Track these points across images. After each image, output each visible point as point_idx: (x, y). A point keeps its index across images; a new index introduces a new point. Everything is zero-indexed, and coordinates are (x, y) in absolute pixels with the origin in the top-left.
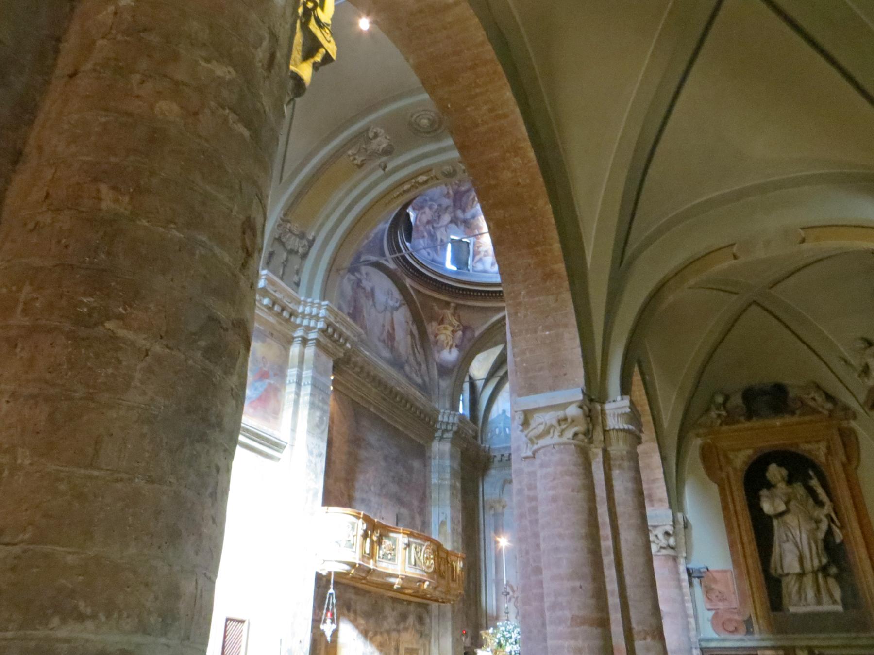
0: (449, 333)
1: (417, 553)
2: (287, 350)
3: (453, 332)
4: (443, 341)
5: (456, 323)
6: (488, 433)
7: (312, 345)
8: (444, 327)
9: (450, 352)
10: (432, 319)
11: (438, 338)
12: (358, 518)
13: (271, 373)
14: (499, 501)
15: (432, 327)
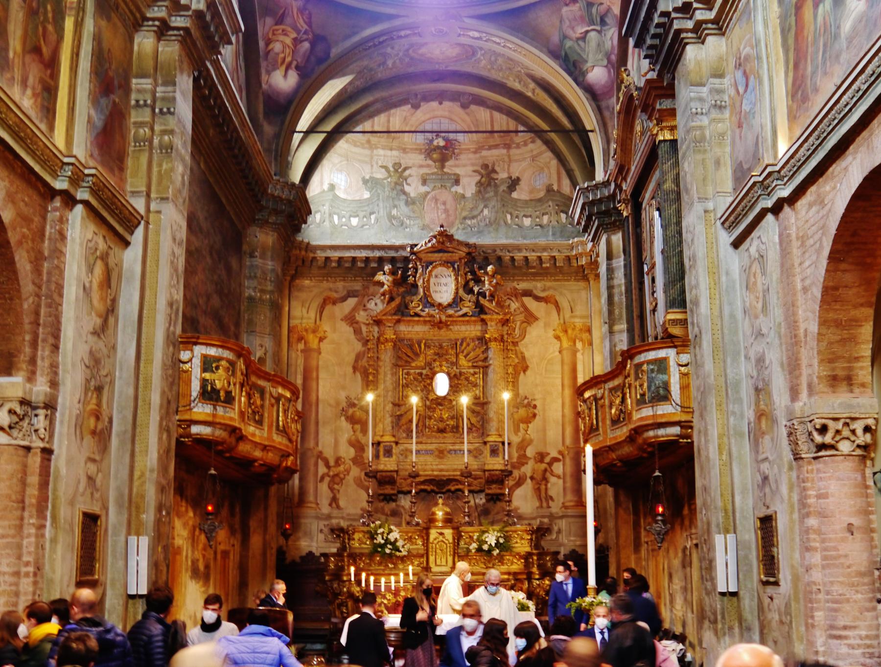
0: (288, 41)
1: (285, 411)
2: (131, 40)
3: (296, 42)
4: (278, 54)
5: (302, 25)
7: (174, 38)
8: (283, 31)
9: (285, 76)
10: (268, 11)
11: (271, 47)
12: (239, 355)
13: (116, 83)
14: (314, 331)
15: (264, 26)
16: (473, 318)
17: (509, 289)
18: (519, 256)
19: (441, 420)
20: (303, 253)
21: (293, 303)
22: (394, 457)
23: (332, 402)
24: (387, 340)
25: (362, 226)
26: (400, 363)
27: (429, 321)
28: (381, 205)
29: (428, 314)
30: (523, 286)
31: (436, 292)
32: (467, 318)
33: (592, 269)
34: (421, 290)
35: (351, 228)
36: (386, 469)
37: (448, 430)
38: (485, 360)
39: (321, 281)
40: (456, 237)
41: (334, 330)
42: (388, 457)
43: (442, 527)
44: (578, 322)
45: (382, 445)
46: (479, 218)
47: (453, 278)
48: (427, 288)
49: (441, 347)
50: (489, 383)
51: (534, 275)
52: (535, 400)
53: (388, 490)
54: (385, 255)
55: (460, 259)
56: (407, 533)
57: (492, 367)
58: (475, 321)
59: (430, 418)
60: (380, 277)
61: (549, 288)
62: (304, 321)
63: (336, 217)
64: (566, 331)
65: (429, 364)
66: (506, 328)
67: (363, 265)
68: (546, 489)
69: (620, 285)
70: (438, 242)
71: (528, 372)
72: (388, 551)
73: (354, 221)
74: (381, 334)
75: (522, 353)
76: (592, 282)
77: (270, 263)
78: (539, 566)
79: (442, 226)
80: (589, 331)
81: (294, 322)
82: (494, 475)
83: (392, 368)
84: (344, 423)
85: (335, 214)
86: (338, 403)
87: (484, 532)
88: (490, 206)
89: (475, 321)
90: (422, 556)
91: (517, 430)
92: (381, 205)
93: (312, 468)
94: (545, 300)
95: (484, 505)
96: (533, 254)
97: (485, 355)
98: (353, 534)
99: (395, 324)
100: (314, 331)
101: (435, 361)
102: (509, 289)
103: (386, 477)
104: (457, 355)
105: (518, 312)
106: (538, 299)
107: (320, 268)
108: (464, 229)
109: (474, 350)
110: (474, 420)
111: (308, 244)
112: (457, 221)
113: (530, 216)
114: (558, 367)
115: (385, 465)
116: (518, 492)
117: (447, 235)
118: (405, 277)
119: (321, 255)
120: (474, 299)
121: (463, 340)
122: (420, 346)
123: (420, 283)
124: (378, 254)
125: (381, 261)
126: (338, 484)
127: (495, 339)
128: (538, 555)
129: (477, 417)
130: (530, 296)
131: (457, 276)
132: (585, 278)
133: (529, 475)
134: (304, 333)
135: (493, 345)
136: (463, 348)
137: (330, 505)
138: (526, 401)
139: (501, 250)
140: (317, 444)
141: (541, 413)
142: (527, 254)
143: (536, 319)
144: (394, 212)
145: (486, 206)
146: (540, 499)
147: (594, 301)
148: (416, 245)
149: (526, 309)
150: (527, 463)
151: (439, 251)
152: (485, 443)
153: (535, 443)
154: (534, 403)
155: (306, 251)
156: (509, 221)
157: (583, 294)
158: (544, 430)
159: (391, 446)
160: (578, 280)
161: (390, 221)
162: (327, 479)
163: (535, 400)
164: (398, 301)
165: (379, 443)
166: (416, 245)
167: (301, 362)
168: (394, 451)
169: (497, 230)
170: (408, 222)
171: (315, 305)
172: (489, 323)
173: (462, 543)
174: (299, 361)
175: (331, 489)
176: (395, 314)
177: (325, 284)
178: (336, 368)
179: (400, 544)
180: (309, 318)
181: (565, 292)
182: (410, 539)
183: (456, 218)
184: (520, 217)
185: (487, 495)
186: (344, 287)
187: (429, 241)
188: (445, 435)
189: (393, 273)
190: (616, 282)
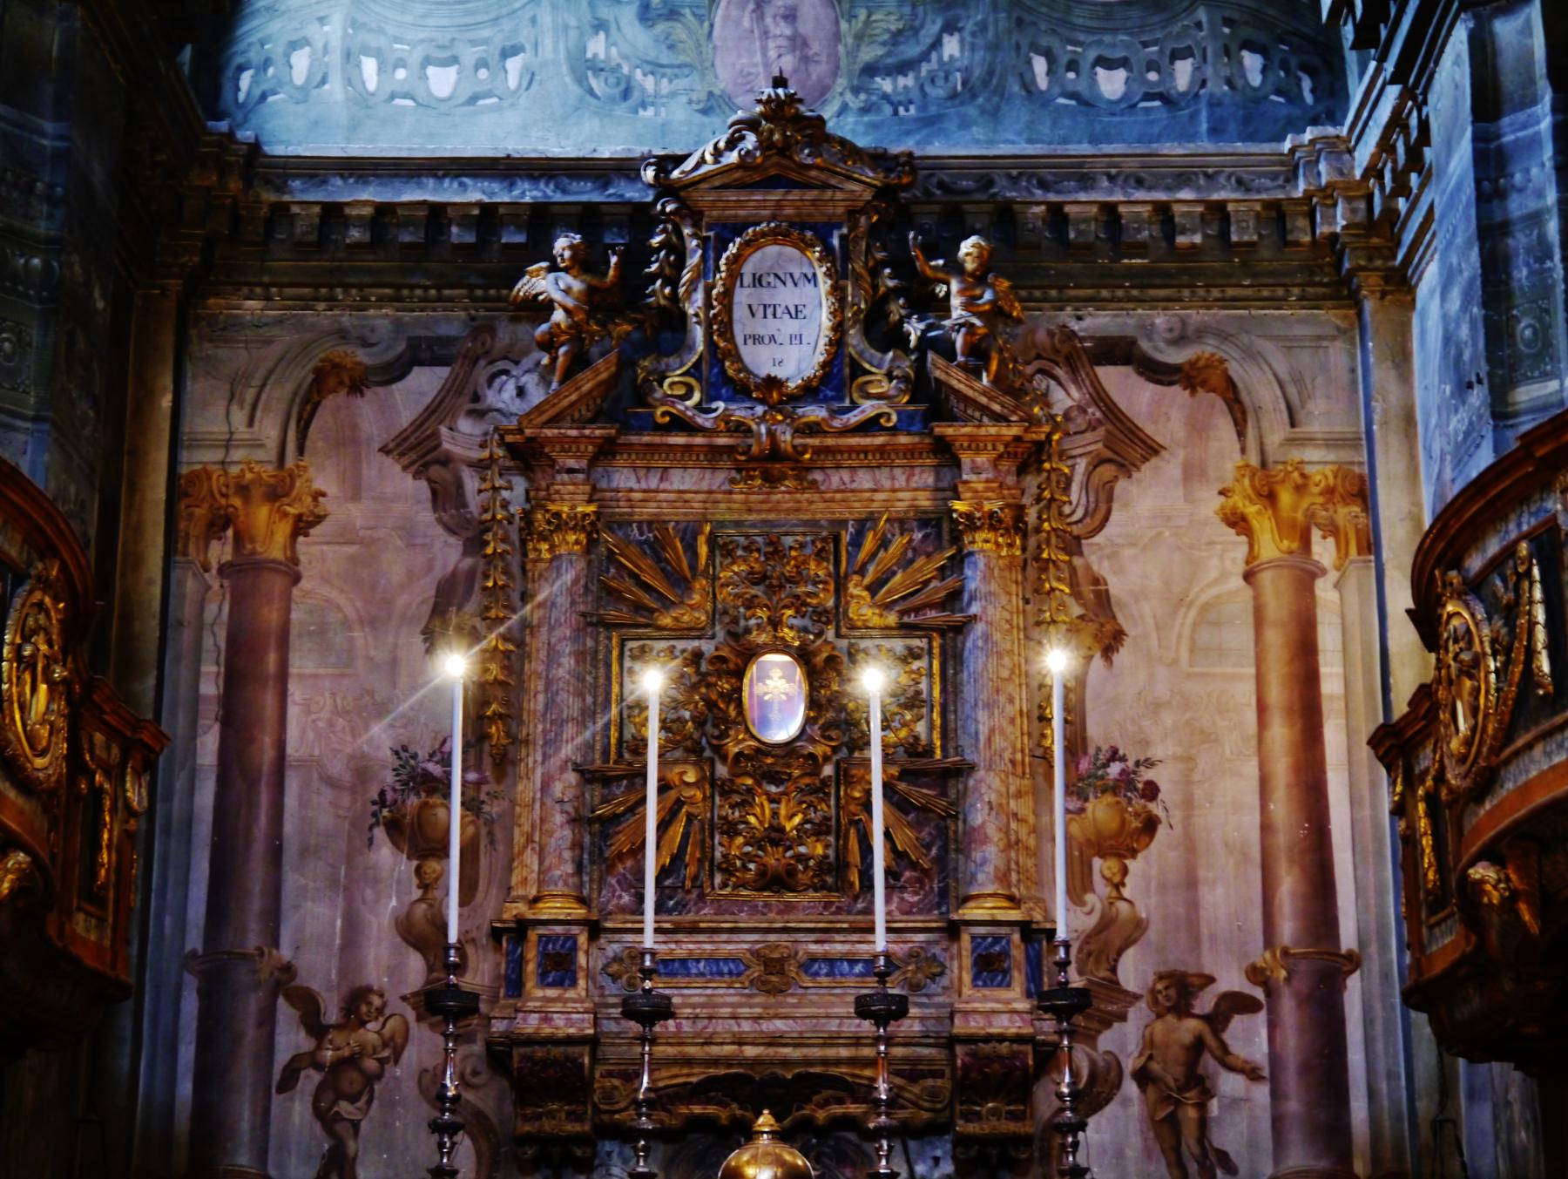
6: (241, 69)
14: (276, 493)
16: (903, 439)
17: (1041, 336)
18: (1082, 202)
19: (775, 836)
20: (235, 184)
21: (196, 387)
22: (582, 983)
23: (338, 767)
24: (559, 524)
25: (473, 99)
26: (612, 613)
27: (730, 450)
28: (546, 19)
29: (725, 418)
30: (1097, 322)
31: (758, 339)
32: (879, 440)
33: (1372, 252)
34: (699, 333)
35: (427, 104)
36: (547, 1030)
37: (803, 878)
38: (954, 597)
39: (307, 303)
40: (832, 126)
41: (355, 491)
42: (555, 984)
44: (1319, 462)
45: (533, 935)
46: (925, 68)
47: (824, 285)
48: (720, 324)
49: (776, 551)
50: (968, 692)
51: (1143, 279)
52: (1150, 763)
53: (559, 1121)
54: (559, 197)
55: (852, 214)
57: (979, 628)
58: (910, 452)
59: (731, 830)
60: (540, 283)
61: (1200, 334)
62: (237, 455)
63: (369, 66)
64: (1270, 498)
66: (1032, 482)
67: (470, 238)
68: (1203, 1123)
69: (1536, 218)
70: (765, 144)
71: (1123, 656)
73: (442, 81)
74: (534, 502)
75: (1096, 581)
76: (1369, 306)
77: (49, 127)
79: (779, 82)
80: (1363, 493)
81: (195, 459)
83: (579, 632)
84: (385, 855)
85: (367, 51)
86: (362, 771)
88: (970, 26)
89: (910, 452)
91: (1079, 885)
92: (546, 19)
94: (1188, 377)
96: (1140, 195)
97: (951, 582)
99: (594, 461)
100: (276, 493)
101: (750, 604)
102: (1041, 336)
103: (548, 1063)
104: (840, 589)
105: (1081, 422)
106: (1156, 372)
107: (302, 249)
108: (865, 110)
109: (905, 563)
110: (905, 837)
111: (256, 147)
112: (841, 83)
113: (1124, 63)
114: (1241, 636)
115: (546, 1018)
116: (1099, 1132)
117: (799, 119)
118: (633, 280)
119: (302, 193)
120: (906, 366)
121: (863, 525)
122: (691, 549)
123: (694, 305)
124: (528, 193)
125: (542, 221)
126: (353, 1099)
127: (993, 522)
129: (917, 826)
130: (1126, 361)
131: (838, 277)
132: (1344, 294)
133: (1129, 1065)
135: (981, 542)
136: (863, 555)
138: (1115, 769)
139: (1014, 180)
140: (276, 943)
141: (1177, 816)
142: (1118, 197)
144: (597, 46)
145: (950, 28)
147: (1382, 375)
148: (681, 159)
149: (1112, 412)
150: (1123, 1018)
151: (769, 183)
152: (953, 930)
153: (1152, 934)
154: (1147, 774)
155: (248, 180)
156: (1042, 82)
157: (1337, 355)
158: (1191, 883)
159: (574, 938)
160: (1313, 302)
161: (581, 80)
162: (310, 1080)
163: (1150, 763)
164: (603, 368)
165: (522, 927)
166: (681, 159)
167: (218, 610)
168: (582, 959)
169: (994, 115)
170: (649, 84)
171: (279, 395)
172: (966, 459)
174: (211, 611)
175: (325, 1117)
177: (322, 316)
180: (257, 445)
181: (1267, 347)
183: (835, 72)
184: (1085, 65)
185: (961, 1141)
186: (398, 325)
187: (732, 144)
188: (790, 897)
189: (584, 262)
190: (1517, 206)
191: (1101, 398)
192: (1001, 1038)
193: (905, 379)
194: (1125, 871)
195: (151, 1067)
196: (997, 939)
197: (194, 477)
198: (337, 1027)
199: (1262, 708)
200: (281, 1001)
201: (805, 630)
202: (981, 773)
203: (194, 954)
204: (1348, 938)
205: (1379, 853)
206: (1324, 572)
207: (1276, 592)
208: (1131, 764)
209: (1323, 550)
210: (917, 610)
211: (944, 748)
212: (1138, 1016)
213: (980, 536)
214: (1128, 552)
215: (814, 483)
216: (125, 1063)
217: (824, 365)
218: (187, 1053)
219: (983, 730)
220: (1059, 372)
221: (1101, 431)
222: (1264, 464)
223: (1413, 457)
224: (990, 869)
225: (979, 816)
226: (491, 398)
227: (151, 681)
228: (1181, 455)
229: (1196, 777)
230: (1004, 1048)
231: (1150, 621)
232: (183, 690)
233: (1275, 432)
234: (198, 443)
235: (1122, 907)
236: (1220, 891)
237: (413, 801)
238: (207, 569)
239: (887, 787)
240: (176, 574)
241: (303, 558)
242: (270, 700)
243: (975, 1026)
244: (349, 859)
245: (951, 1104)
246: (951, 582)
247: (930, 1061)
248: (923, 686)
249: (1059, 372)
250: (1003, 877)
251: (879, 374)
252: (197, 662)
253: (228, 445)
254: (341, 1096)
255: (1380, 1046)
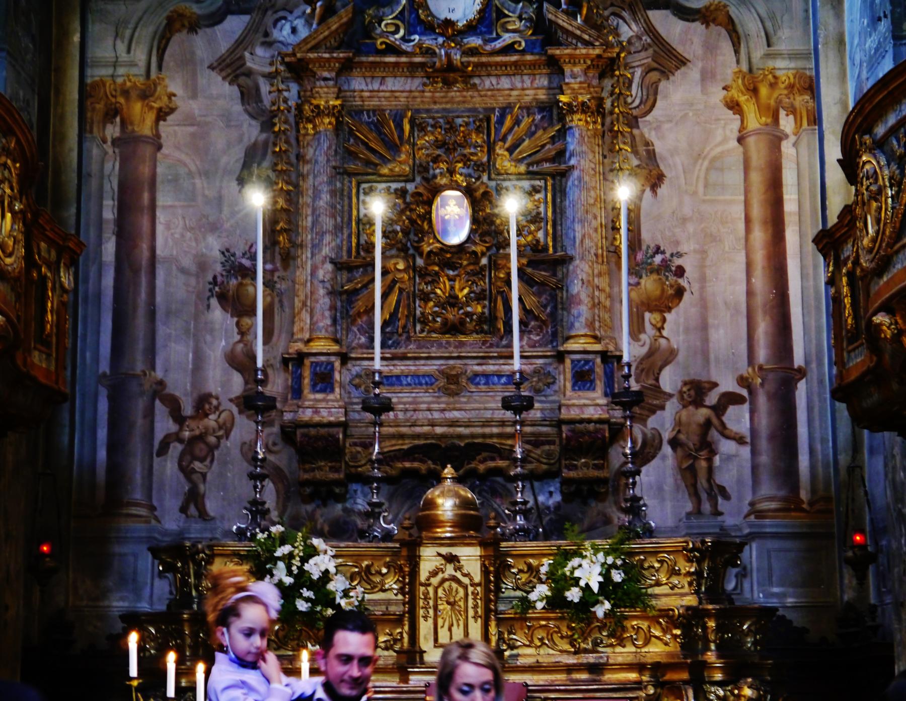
14: (146, 95)
16: (529, 58)
19: (452, 301)
21: (95, 28)
22: (337, 390)
23: (187, 262)
24: (319, 112)
26: (352, 166)
27: (422, 65)
29: (420, 45)
32: (514, 58)
36: (317, 418)
37: (470, 326)
38: (560, 155)
42: (322, 391)
43: (453, 542)
44: (785, 68)
45: (307, 362)
49: (451, 128)
50: (569, 213)
52: (679, 255)
53: (325, 472)
56: (357, 558)
57: (576, 173)
58: (533, 65)
59: (425, 298)
62: (121, 71)
65: (422, 169)
66: (608, 83)
68: (710, 470)
71: (663, 190)
72: (302, 606)
74: (304, 98)
75: (647, 144)
78: (721, 652)
80: (812, 87)
81: (95, 74)
82: (583, 433)
84: (218, 314)
86: (202, 265)
87: (567, 556)
89: (533, 65)
90: (399, 621)
91: (637, 329)
93: (140, 422)
94: (705, 16)
95: (558, 507)
97: (558, 145)
98: (210, 560)
99: (339, 73)
100: (146, 95)
101: (436, 160)
103: (318, 438)
104: (491, 151)
105: (638, 45)
109: (531, 134)
110: (531, 302)
114: (735, 177)
115: (316, 411)
116: (648, 475)
121: (505, 110)
122: (399, 127)
126: (202, 460)
127: (584, 108)
128: (717, 616)
129: (538, 294)
133: (666, 436)
134: (122, 100)
135: (577, 121)
136: (504, 130)
137: (184, 509)
138: (658, 259)
140: (153, 367)
141: (696, 287)
143: (683, 62)
146: (695, 494)
150: (662, 408)
152: (560, 357)
153: (680, 357)
154: (678, 262)
158: (704, 327)
159: (331, 364)
162: (176, 449)
163: (679, 255)
164: (344, 15)
165: (301, 357)
167: (112, 167)
168: (337, 376)
171: (146, 33)
172: (567, 69)
173: (508, 583)
174: (108, 166)
175: (186, 471)
176: (338, 48)
178: (198, 182)
179: (337, 585)
180: (133, 64)
182: (365, 576)
185: (565, 482)
188: (462, 338)
191: (651, 30)
192: (589, 421)
193: (530, 19)
194: (664, 320)
195: (81, 441)
196: (587, 362)
197: (95, 85)
198: (192, 418)
199: (748, 220)
200: (158, 403)
201: (470, 176)
202: (577, 262)
203: (104, 375)
204: (799, 359)
205: (818, 308)
206: (787, 136)
207: (757, 149)
208: (668, 255)
209: (787, 123)
210: (538, 163)
211: (554, 247)
212: (672, 407)
213: (576, 117)
214: (666, 126)
215: (475, 85)
216: (66, 439)
217: (480, 12)
218: (102, 434)
219: (578, 236)
220: (625, 14)
221: (651, 51)
222: (751, 70)
223: (843, 64)
224: (582, 319)
225: (576, 288)
226: (276, 34)
227: (73, 210)
228: (700, 64)
229: (708, 263)
230: (591, 426)
231: (680, 168)
232: (93, 216)
233: (758, 50)
234: (97, 64)
235: (663, 342)
236: (722, 331)
237: (233, 282)
238: (104, 141)
239: (520, 270)
240: (86, 145)
241: (163, 135)
242: (145, 222)
243: (574, 413)
244: (196, 317)
245: (559, 460)
246: (558, 145)
247: (547, 435)
248: (542, 209)
249: (625, 14)
250: (590, 325)
251: (514, 17)
252: (101, 198)
253: (115, 65)
254: (195, 458)
255: (817, 423)
